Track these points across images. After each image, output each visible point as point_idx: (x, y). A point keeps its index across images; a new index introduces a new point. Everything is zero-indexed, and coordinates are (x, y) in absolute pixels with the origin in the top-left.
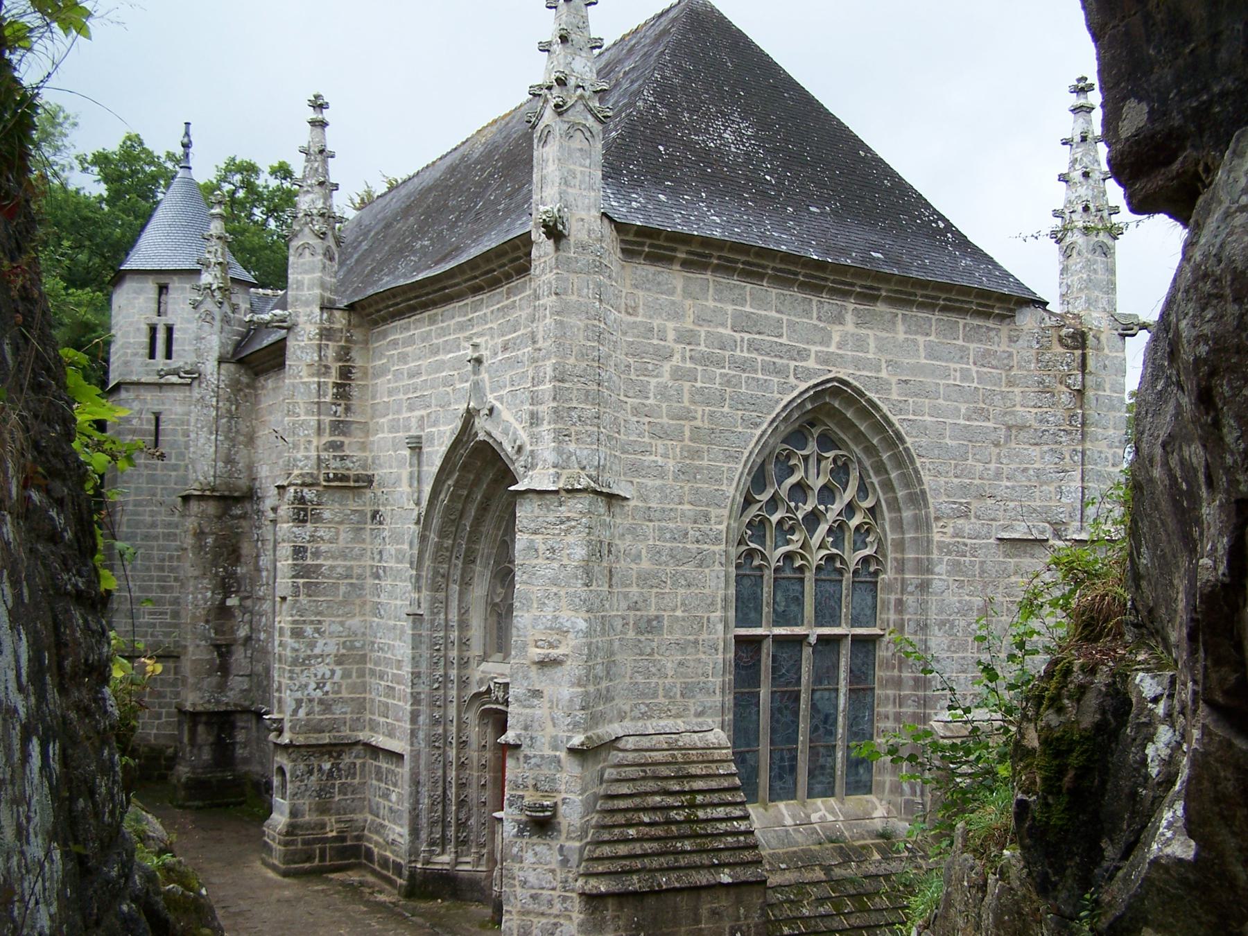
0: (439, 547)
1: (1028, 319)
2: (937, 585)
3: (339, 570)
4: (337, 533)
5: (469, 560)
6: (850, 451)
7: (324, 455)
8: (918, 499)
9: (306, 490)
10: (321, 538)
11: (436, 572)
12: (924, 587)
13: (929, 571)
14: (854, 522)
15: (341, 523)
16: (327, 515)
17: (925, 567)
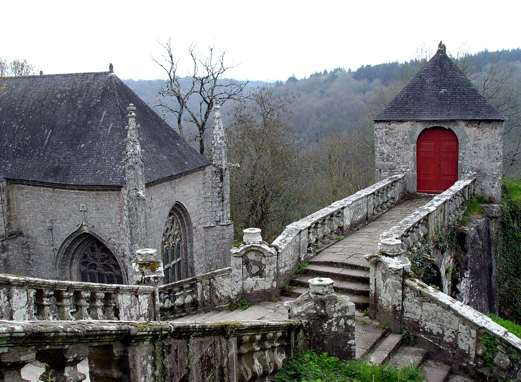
0: (63, 257)
1: (208, 169)
2: (194, 244)
3: (15, 263)
4: (13, 252)
5: (72, 259)
6: (174, 215)
7: (7, 229)
8: (189, 224)
9: (4, 242)
10: (9, 255)
11: (62, 265)
12: (192, 246)
13: (193, 241)
14: (176, 233)
15: (14, 249)
16: (10, 247)
17: (191, 241)
